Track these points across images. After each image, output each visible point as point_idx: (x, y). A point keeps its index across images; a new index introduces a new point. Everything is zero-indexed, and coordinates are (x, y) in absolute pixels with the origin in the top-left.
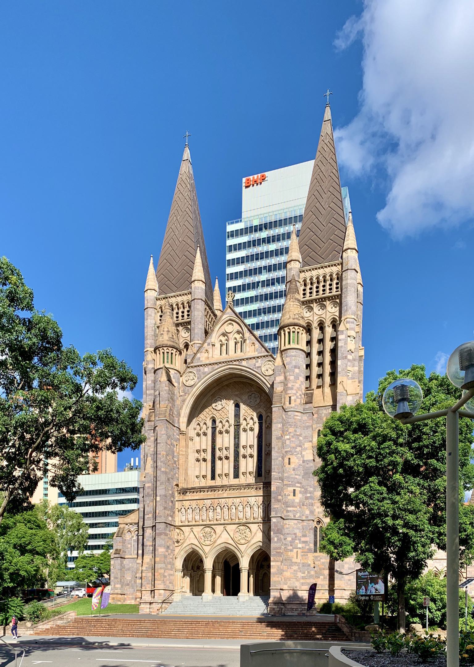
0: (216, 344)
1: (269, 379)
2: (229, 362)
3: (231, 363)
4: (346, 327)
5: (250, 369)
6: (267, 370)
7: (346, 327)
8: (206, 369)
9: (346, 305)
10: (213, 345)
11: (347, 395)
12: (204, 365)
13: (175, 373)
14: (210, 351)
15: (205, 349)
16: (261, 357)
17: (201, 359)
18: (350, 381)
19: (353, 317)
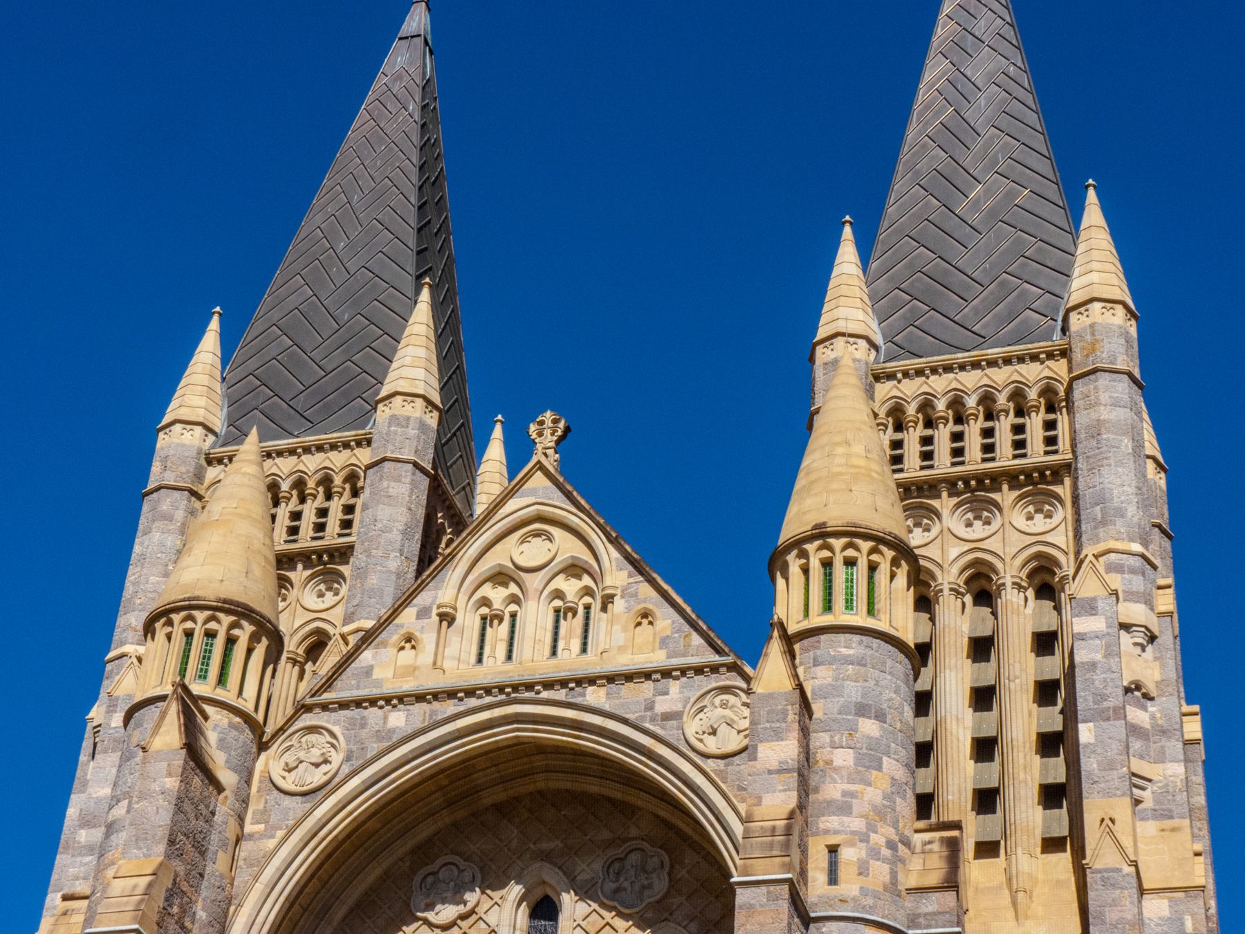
0: (459, 617)
1: (717, 772)
2: (515, 688)
3: (528, 695)
4: (1105, 585)
5: (625, 721)
6: (714, 732)
7: (1105, 585)
8: (398, 719)
9: (1101, 500)
10: (447, 618)
11: (1142, 891)
12: (388, 700)
13: (232, 726)
14: (428, 639)
15: (403, 631)
16: (683, 672)
17: (377, 674)
18: (1149, 828)
19: (1137, 547)
